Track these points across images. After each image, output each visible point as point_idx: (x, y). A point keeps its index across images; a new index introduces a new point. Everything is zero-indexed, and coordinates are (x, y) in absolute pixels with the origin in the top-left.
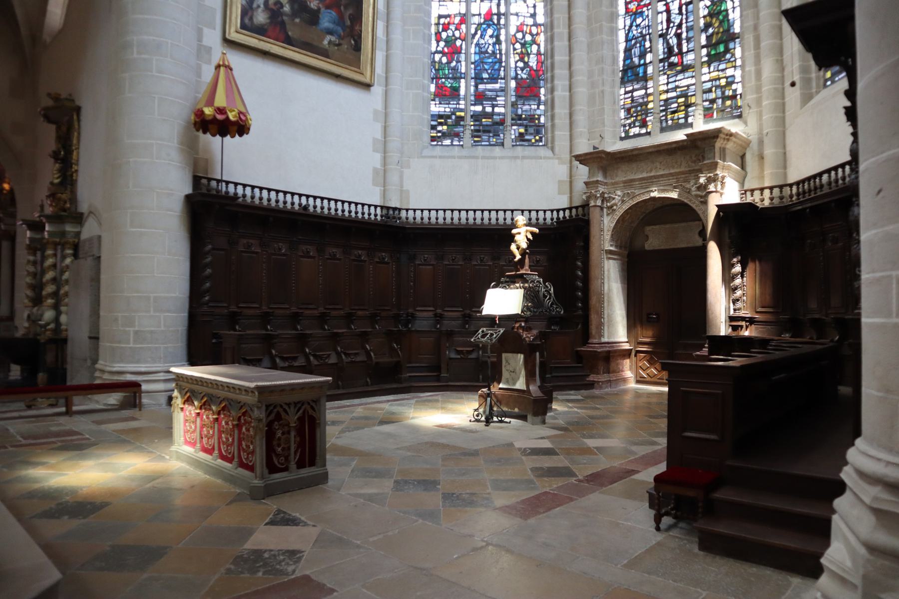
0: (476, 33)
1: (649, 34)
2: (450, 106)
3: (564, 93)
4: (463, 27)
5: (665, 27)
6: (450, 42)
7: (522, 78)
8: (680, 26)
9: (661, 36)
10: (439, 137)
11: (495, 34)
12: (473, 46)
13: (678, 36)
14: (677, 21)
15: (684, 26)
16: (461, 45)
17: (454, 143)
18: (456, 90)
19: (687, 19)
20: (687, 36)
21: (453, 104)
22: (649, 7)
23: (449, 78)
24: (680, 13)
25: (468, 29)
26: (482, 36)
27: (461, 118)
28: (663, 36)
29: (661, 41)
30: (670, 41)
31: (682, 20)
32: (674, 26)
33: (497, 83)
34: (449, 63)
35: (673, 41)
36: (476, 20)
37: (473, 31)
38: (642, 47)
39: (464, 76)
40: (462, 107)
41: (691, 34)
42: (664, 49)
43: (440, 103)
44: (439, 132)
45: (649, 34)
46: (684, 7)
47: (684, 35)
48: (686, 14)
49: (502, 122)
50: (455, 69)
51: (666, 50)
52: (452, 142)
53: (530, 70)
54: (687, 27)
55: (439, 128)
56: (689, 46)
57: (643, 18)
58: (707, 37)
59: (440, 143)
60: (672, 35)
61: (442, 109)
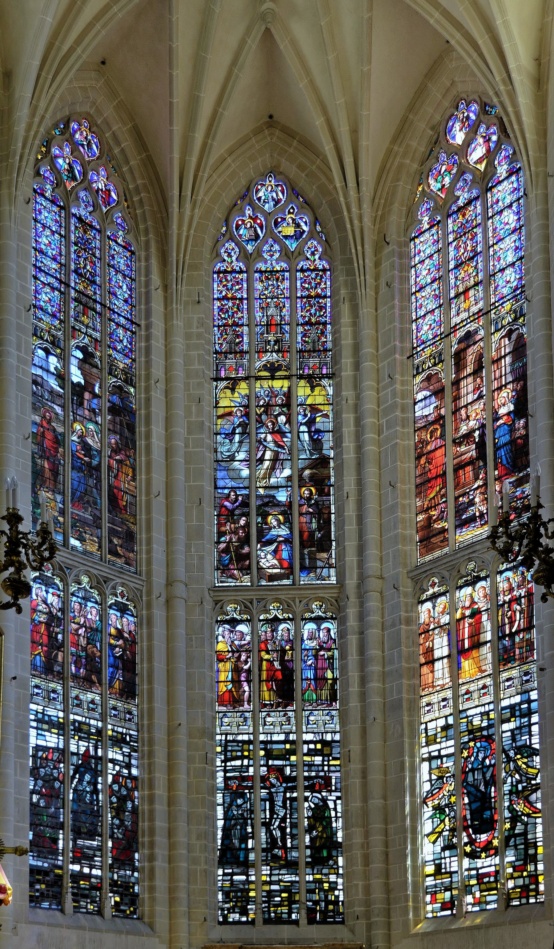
0: (73, 777)
1: (252, 819)
2: (49, 861)
3: (164, 864)
4: (62, 765)
5: (268, 816)
6: (49, 781)
7: (118, 838)
8: (283, 820)
9: (264, 824)
10: (37, 897)
11: (93, 781)
12: (72, 791)
13: (282, 830)
14: (282, 814)
15: (288, 820)
16: (60, 787)
17: (53, 907)
18: (55, 841)
19: (291, 815)
20: (291, 831)
21: (52, 859)
22: (252, 791)
23: (47, 826)
24: (284, 806)
25: (67, 768)
26: (81, 781)
27: (60, 877)
28: (267, 825)
29: (264, 830)
30: (274, 832)
31: (286, 814)
32: (277, 818)
33: (94, 840)
34: (47, 807)
35: (277, 833)
36: (74, 759)
37: (71, 772)
38: (243, 831)
39: (62, 826)
40: (60, 863)
41: (295, 832)
42: (267, 839)
43: (38, 856)
44: (37, 890)
45: (252, 819)
46: (288, 802)
47: (288, 830)
48: (290, 810)
49: (98, 888)
50: (55, 816)
51: (269, 840)
52: (50, 905)
53: (126, 830)
54: (291, 822)
55: (38, 887)
56: (293, 843)
57: (244, 799)
58: (311, 839)
59: (38, 905)
60: (275, 827)
61: (40, 864)
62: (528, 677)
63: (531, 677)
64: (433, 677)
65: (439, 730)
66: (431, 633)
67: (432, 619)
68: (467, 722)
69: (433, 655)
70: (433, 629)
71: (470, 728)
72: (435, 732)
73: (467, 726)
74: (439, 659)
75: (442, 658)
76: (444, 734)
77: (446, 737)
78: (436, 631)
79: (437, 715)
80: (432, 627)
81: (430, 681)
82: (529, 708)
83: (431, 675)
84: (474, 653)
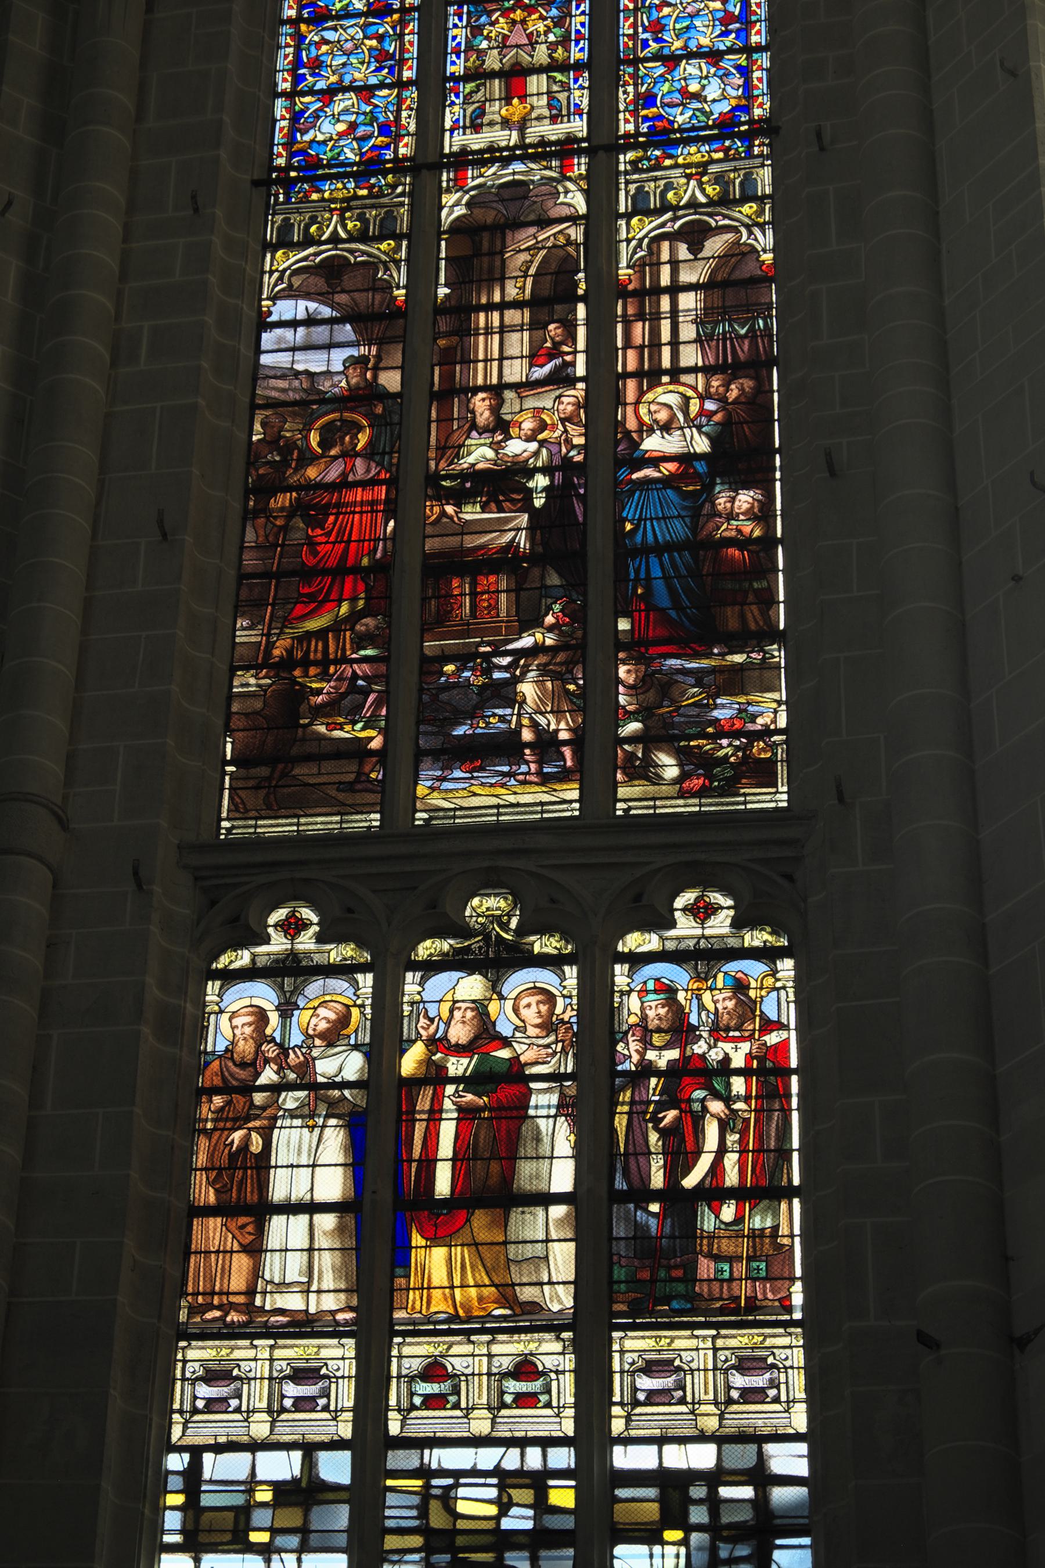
62: (759, 1381)
63: (774, 1384)
64: (256, 1273)
65: (264, 1495)
66: (259, 1098)
67: (270, 1051)
68: (425, 1494)
69: (263, 1185)
70: (275, 1089)
71: (438, 1519)
72: (239, 1500)
73: (423, 1511)
74: (290, 1208)
75: (312, 1208)
76: (292, 1517)
77: (304, 1531)
78: (291, 1100)
79: (260, 1429)
80: (268, 1076)
81: (238, 1282)
82: (761, 1502)
83: (241, 1263)
84: (480, 1223)
